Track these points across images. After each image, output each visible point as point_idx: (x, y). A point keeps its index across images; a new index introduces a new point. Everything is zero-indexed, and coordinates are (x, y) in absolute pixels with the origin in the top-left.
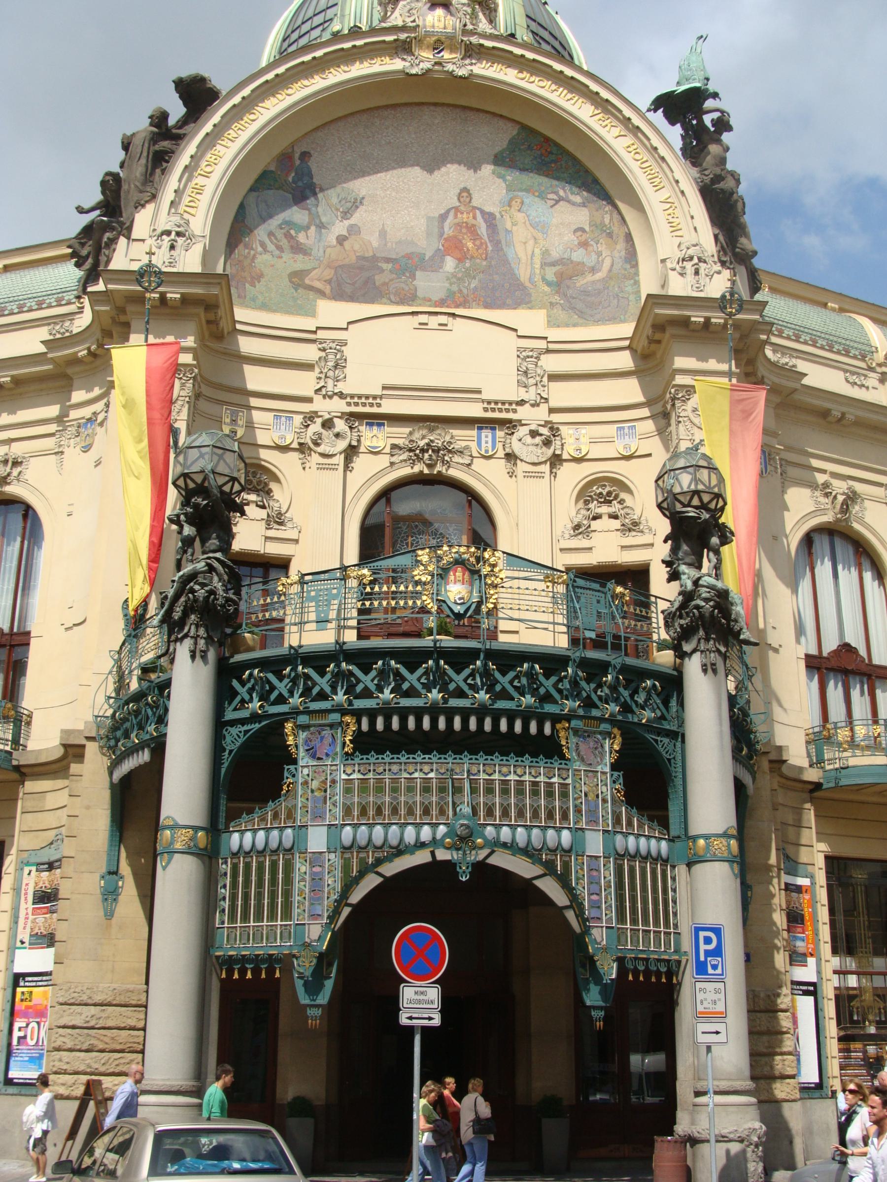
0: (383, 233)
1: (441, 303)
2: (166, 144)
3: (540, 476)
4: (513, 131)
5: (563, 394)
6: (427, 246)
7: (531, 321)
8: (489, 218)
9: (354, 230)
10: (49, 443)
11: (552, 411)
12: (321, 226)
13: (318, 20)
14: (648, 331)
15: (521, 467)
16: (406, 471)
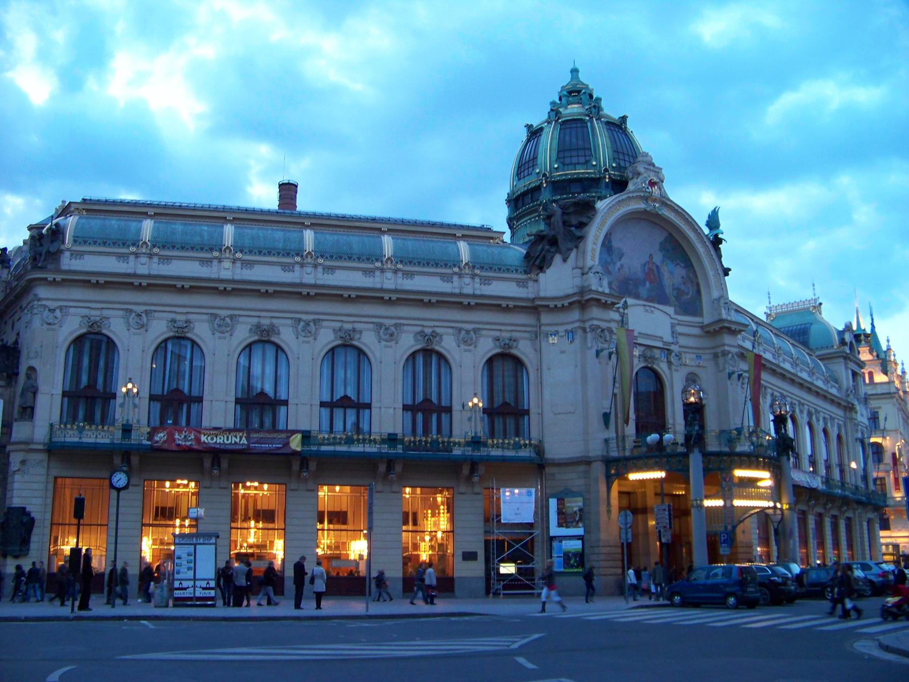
0: (629, 269)
1: (646, 300)
2: (566, 217)
3: (677, 370)
4: (665, 234)
5: (683, 341)
6: (641, 275)
7: (670, 310)
8: (657, 267)
9: (622, 266)
10: (527, 335)
11: (680, 347)
12: (614, 264)
13: (581, 153)
14: (717, 327)
15: (673, 367)
16: (643, 365)
